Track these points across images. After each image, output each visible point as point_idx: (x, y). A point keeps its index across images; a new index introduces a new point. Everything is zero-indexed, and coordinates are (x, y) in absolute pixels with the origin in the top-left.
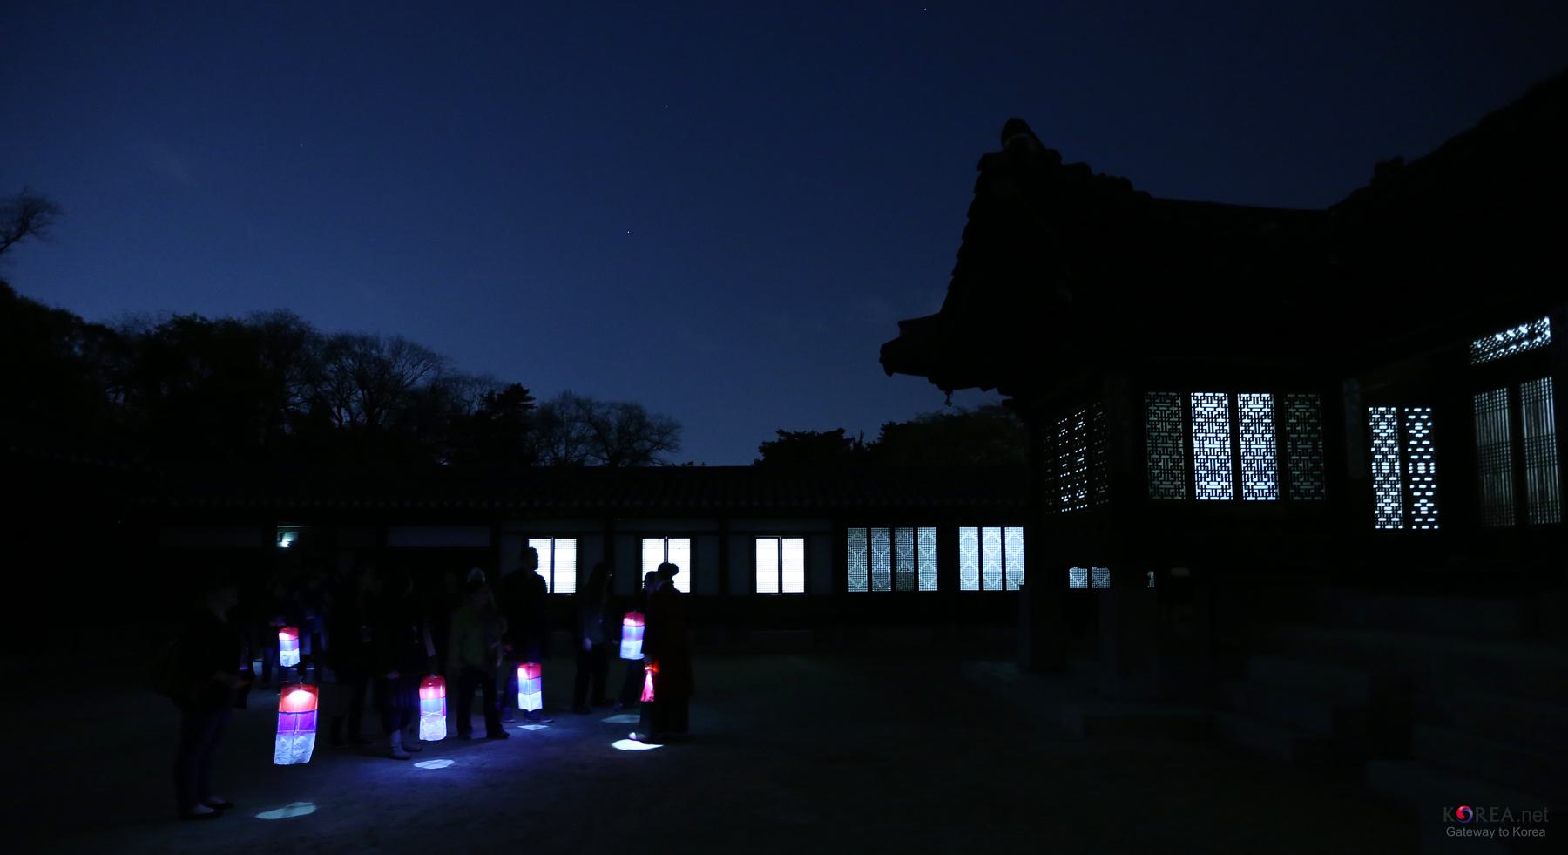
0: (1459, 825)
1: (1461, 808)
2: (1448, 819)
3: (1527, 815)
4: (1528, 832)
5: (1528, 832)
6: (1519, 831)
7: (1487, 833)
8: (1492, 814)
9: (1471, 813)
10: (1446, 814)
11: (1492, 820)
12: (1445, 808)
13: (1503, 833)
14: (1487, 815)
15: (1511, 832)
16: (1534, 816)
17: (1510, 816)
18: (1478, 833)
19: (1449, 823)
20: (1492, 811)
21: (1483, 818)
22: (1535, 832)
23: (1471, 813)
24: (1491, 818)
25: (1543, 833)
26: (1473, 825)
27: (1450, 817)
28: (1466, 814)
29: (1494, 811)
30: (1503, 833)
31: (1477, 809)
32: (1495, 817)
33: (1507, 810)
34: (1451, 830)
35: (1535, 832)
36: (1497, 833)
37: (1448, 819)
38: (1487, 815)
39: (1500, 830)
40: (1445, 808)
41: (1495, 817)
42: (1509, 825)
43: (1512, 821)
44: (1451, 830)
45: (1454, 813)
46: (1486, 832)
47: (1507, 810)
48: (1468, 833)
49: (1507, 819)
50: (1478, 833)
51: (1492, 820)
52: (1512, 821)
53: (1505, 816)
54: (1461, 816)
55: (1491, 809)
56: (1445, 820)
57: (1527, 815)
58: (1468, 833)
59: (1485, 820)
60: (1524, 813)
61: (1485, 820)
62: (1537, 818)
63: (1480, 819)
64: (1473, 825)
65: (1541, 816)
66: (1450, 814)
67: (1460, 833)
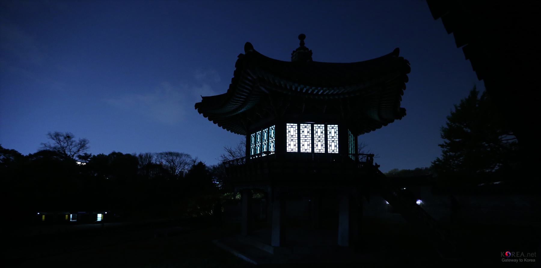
0: (506, 258)
1: (507, 252)
2: (502, 256)
3: (529, 255)
4: (529, 260)
5: (529, 260)
6: (526, 260)
7: (515, 260)
8: (517, 254)
9: (510, 254)
10: (502, 254)
11: (517, 256)
12: (501, 252)
13: (521, 260)
14: (515, 255)
15: (524, 260)
16: (531, 255)
17: (523, 255)
18: (512, 260)
19: (503, 257)
20: (517, 253)
21: (514, 255)
22: (532, 260)
23: (510, 254)
24: (517, 255)
25: (534, 260)
26: (511, 258)
27: (503, 256)
28: (509, 254)
29: (518, 253)
30: (521, 260)
31: (512, 252)
32: (518, 255)
33: (522, 253)
34: (503, 260)
35: (532, 260)
36: (519, 260)
37: (502, 256)
38: (515, 255)
39: (520, 259)
40: (501, 252)
41: (518, 256)
42: (523, 258)
43: (524, 256)
44: (503, 260)
45: (504, 254)
46: (515, 260)
47: (522, 253)
48: (509, 260)
49: (522, 256)
50: (512, 260)
51: (517, 256)
52: (524, 256)
53: (521, 255)
54: (507, 255)
55: (517, 252)
56: (501, 256)
57: (529, 255)
58: (509, 260)
59: (515, 256)
60: (528, 254)
61: (515, 256)
62: (532, 256)
63: (513, 255)
64: (511, 258)
65: (534, 255)
66: (503, 254)
67: (506, 260)
